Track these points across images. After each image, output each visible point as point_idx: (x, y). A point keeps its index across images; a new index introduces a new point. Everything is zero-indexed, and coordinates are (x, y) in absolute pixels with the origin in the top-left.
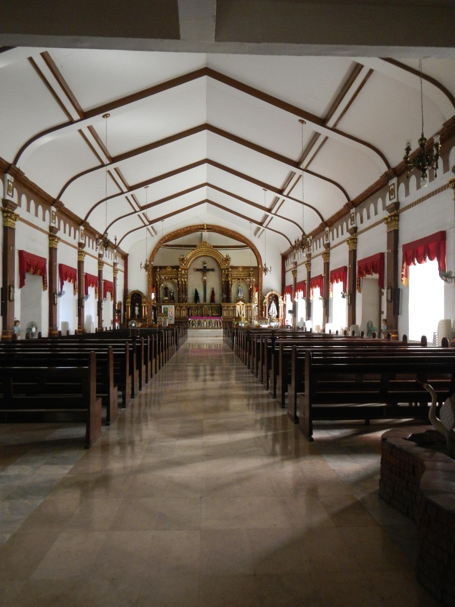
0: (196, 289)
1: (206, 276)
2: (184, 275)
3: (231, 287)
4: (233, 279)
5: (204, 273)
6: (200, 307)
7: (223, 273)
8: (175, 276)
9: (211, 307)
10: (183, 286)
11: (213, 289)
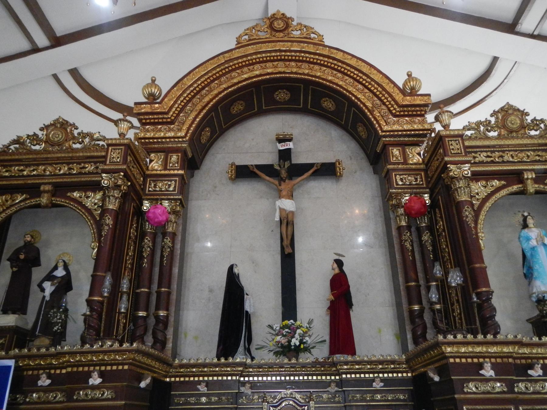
0: (231, 268)
1: (291, 196)
2: (158, 177)
3: (476, 227)
4: (476, 176)
5: (281, 180)
6: (253, 385)
7: (393, 160)
8: (90, 173)
9: (341, 383)
10: (147, 241)
11: (339, 263)
